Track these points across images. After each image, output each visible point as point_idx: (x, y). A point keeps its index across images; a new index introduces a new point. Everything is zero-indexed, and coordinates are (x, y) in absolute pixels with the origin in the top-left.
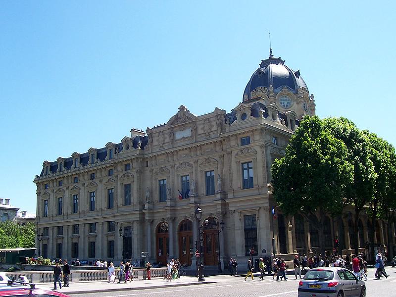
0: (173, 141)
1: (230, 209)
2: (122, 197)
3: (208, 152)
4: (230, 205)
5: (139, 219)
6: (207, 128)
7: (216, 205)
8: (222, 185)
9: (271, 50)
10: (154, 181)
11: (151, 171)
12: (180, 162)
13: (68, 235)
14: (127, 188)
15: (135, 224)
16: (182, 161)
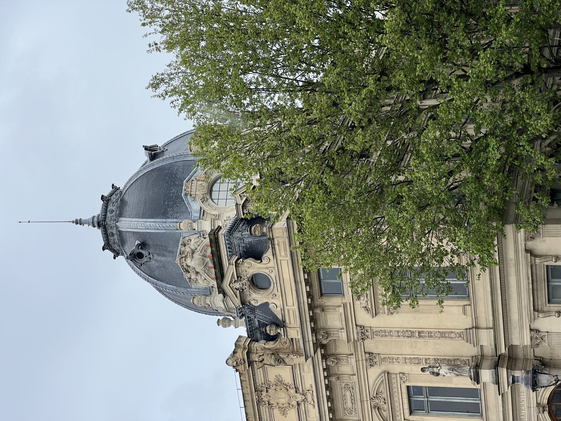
4: (516, 342)
6: (282, 398)
8: (455, 365)
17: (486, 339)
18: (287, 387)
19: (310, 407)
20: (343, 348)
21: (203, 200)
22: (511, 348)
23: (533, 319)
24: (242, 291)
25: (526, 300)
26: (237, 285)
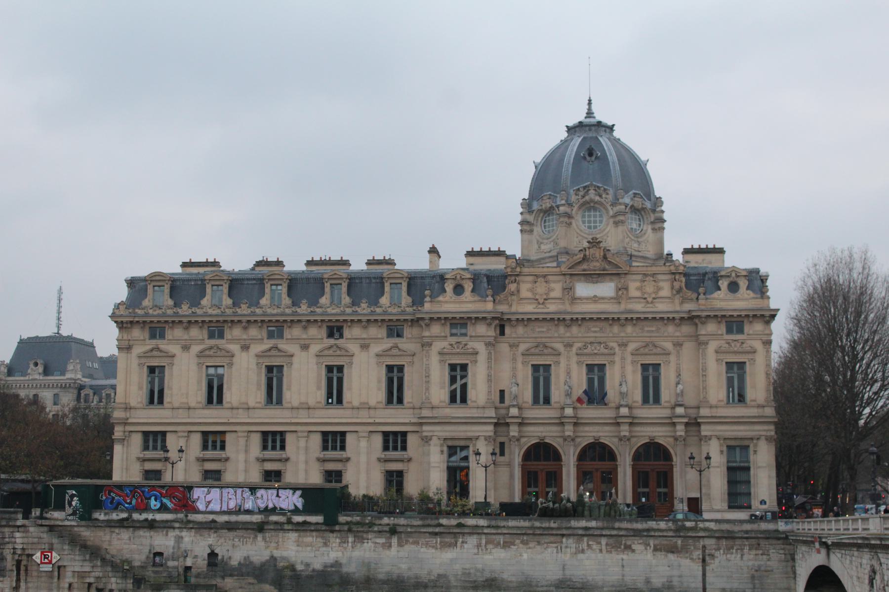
0: (574, 300)
2: (442, 388)
3: (648, 331)
5: (492, 434)
7: (674, 424)
9: (590, 101)
11: (513, 346)
14: (458, 372)
16: (592, 340)
17: (704, 412)
18: (656, 292)
19: (643, 305)
20: (686, 329)
21: (632, 206)
22: (699, 424)
24: (728, 276)
26: (733, 275)
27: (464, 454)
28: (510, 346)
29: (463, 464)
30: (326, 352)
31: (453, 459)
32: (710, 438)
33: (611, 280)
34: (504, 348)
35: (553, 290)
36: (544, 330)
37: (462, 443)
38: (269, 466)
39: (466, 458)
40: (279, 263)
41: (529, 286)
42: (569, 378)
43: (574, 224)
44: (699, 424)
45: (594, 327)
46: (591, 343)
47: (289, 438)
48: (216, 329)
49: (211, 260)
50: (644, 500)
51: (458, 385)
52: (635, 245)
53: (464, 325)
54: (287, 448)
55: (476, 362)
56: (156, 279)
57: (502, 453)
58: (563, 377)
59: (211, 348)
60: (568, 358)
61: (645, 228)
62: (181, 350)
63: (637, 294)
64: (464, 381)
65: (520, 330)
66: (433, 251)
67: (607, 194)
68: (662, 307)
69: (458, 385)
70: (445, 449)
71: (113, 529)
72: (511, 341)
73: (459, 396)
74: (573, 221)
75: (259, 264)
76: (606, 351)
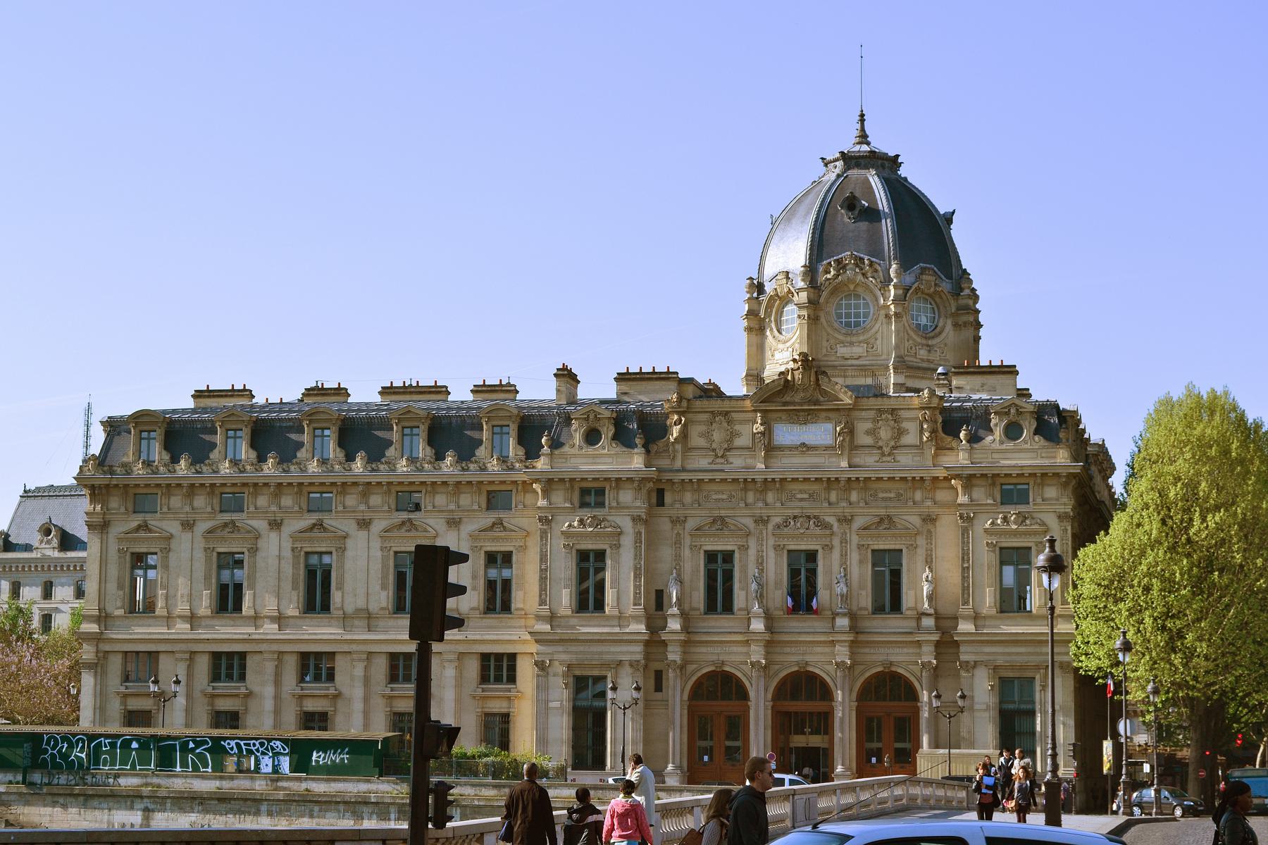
1: (963, 657)
3: (884, 499)
4: (962, 649)
5: (639, 657)
7: (919, 644)
9: (862, 115)
10: (687, 553)
11: (676, 521)
12: (790, 512)
13: (277, 682)
15: (626, 672)
16: (796, 512)
21: (917, 289)
23: (985, 664)
25: (1000, 661)
26: (1013, 411)
27: (599, 688)
28: (672, 522)
29: (597, 703)
30: (395, 533)
31: (583, 695)
32: (971, 667)
33: (828, 419)
34: (665, 525)
35: (739, 434)
36: (724, 497)
37: (596, 673)
38: (311, 706)
39: (603, 695)
40: (341, 392)
41: (702, 428)
42: (761, 570)
43: (823, 320)
44: (957, 644)
45: (801, 492)
46: (795, 517)
47: (340, 664)
48: (230, 498)
49: (239, 387)
50: (706, 758)
51: (590, 583)
52: (923, 353)
53: (601, 492)
54: (337, 678)
55: (618, 546)
56: (143, 420)
57: (659, 687)
58: (753, 570)
59: (226, 525)
60: (760, 541)
61: (941, 324)
62: (180, 528)
63: (868, 440)
64: (599, 576)
65: (688, 497)
66: (566, 376)
67: (876, 271)
68: (906, 460)
69: (590, 583)
70: (571, 680)
71: (56, 799)
72: (673, 513)
73: (590, 599)
74: (822, 314)
75: (309, 392)
76: (818, 531)
